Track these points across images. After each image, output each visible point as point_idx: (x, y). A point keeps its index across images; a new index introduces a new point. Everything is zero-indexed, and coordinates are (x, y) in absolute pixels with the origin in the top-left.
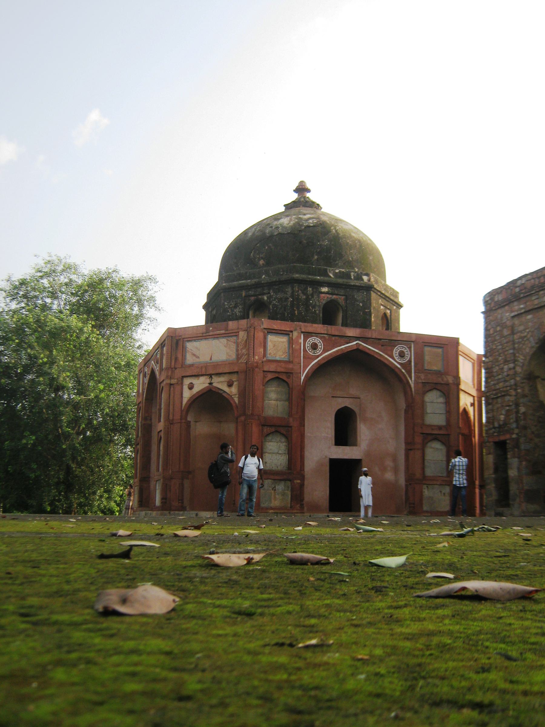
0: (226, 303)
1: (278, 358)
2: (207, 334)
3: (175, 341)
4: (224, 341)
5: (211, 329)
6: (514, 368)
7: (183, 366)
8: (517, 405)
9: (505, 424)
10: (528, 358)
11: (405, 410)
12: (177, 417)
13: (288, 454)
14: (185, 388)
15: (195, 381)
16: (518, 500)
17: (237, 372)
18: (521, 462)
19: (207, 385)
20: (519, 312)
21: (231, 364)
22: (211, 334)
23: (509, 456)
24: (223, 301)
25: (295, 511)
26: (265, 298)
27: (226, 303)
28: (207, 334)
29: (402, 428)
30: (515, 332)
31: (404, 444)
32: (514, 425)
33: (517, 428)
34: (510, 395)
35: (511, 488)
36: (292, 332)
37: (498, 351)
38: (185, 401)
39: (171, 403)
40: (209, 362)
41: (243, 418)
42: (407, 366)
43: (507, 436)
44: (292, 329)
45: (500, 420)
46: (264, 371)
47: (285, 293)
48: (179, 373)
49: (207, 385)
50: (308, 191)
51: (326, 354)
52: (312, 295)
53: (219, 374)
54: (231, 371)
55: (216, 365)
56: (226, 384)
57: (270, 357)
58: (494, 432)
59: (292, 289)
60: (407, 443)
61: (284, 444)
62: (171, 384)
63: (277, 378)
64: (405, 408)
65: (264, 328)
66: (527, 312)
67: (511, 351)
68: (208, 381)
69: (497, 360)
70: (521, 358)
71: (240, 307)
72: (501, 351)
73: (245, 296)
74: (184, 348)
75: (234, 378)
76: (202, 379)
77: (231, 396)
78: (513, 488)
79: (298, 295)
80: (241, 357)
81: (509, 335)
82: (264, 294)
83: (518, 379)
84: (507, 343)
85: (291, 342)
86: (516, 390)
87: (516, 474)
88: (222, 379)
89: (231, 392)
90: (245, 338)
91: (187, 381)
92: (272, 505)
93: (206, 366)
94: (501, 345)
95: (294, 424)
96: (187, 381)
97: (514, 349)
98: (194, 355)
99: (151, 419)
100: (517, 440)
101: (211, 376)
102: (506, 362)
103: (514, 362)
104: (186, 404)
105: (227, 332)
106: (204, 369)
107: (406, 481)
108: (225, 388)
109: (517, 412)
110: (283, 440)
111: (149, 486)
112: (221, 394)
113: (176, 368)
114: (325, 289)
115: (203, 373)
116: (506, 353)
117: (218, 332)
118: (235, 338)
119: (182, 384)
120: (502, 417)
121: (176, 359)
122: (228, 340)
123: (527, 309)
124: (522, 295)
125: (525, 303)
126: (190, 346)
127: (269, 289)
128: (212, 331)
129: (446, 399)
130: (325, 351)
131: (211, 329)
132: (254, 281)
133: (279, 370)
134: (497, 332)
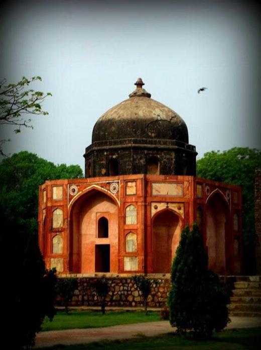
4: (175, 185)
15: (158, 205)
17: (183, 203)
21: (180, 198)
22: (168, 180)
26: (159, 156)
38: (152, 215)
42: (229, 200)
55: (171, 198)
68: (166, 205)
74: (151, 187)
75: (182, 205)
76: (162, 204)
80: (186, 195)
82: (158, 154)
85: (203, 188)
90: (188, 185)
91: (153, 205)
101: (167, 203)
119: (151, 206)
126: (154, 185)
127: (161, 152)
128: (169, 179)
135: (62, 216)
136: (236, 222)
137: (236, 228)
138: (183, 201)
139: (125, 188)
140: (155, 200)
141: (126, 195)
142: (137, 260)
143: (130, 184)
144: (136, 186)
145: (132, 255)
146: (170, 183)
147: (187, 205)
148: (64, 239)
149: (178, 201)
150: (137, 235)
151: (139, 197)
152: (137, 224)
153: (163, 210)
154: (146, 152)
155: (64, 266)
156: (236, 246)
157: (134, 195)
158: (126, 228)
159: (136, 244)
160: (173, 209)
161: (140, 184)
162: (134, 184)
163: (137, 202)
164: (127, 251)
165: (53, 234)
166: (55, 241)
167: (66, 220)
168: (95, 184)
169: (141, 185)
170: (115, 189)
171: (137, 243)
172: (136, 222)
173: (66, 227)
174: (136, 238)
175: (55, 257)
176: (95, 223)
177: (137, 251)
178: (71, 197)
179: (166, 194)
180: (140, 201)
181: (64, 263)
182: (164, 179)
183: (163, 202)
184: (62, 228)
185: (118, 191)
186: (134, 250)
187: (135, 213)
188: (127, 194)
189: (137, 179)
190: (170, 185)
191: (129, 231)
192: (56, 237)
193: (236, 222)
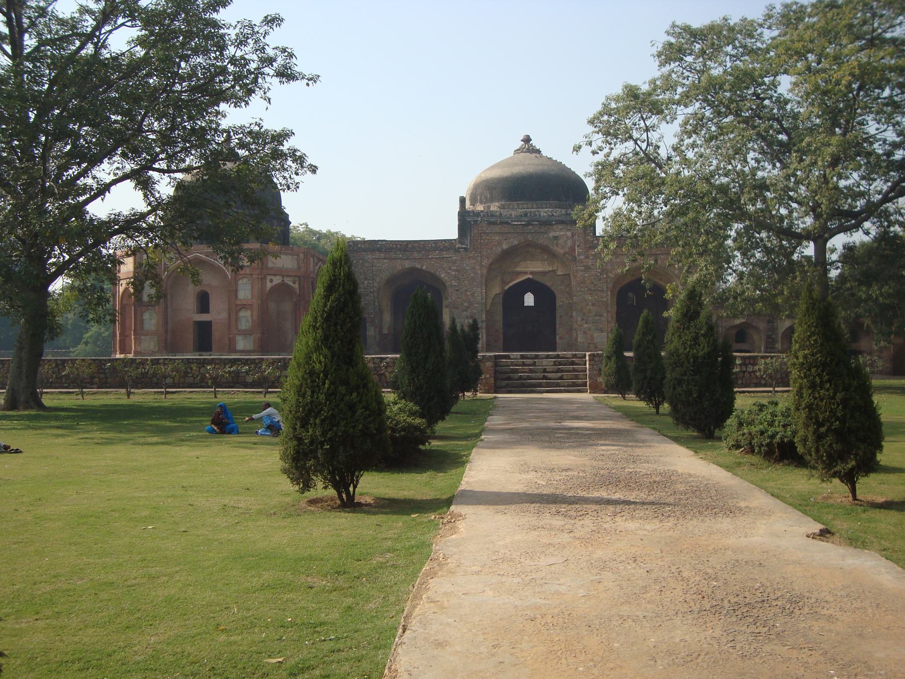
15: (272, 277)
38: (268, 289)
53: (288, 276)
70: (378, 279)
76: (278, 277)
91: (269, 278)
96: (269, 278)
102: (366, 279)
108: (291, 284)
142: (252, 338)
145: (246, 333)
150: (252, 311)
158: (238, 303)
172: (250, 297)
187: (249, 287)
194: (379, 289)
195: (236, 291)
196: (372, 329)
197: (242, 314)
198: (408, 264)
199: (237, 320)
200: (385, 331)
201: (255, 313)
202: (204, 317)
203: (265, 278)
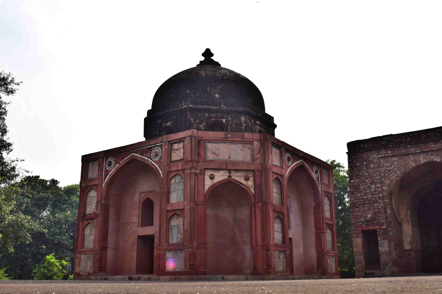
0: (192, 119)
1: (276, 164)
2: (226, 139)
3: (197, 141)
4: (241, 146)
5: (229, 136)
6: (381, 187)
7: (205, 161)
8: (385, 209)
9: (373, 219)
10: (394, 182)
11: (315, 208)
12: (201, 199)
13: (283, 232)
14: (207, 178)
15: (216, 174)
16: (389, 265)
17: (253, 171)
18: (389, 243)
19: (227, 177)
20: (386, 155)
21: (248, 163)
23: (379, 239)
24: (189, 117)
25: (288, 274)
26: (224, 121)
27: (192, 119)
28: (226, 139)
29: (312, 219)
30: (381, 166)
31: (314, 230)
32: (384, 221)
33: (386, 222)
34: (379, 203)
35: (381, 258)
36: (281, 147)
37: (365, 176)
39: (196, 188)
40: (228, 160)
41: (260, 205)
42: (318, 178)
43: (377, 227)
44: (282, 146)
45: (367, 217)
46: (273, 172)
47: (240, 120)
48: (202, 165)
49: (227, 177)
50: (212, 55)
51: (293, 165)
52: (254, 125)
53: (237, 170)
54: (249, 169)
55: (235, 163)
56: (243, 178)
57: (274, 163)
58: (362, 224)
59: (246, 118)
60: (315, 228)
61: (280, 225)
62: (195, 174)
63: (277, 179)
64: (314, 206)
65: (272, 142)
66: (393, 156)
67: (379, 177)
68: (228, 174)
69: (364, 182)
71: (204, 124)
72: (367, 176)
73: (208, 117)
74: (205, 147)
76: (222, 173)
77: (248, 187)
78: (383, 258)
79: (248, 123)
80: (256, 160)
81: (376, 167)
82: (224, 118)
83: (385, 194)
84: (374, 172)
86: (383, 200)
87: (387, 249)
88: (239, 174)
89: (248, 185)
90: (259, 146)
91: (208, 173)
92: (279, 270)
93: (226, 163)
94: (367, 173)
95: (285, 212)
97: (381, 176)
98: (215, 153)
99: (109, 200)
100: (387, 229)
101: (230, 171)
102: (372, 183)
103: (381, 184)
104: (208, 190)
105: (243, 140)
106: (224, 165)
107: (317, 253)
109: (386, 213)
110: (280, 222)
111: (107, 254)
112: (239, 185)
113: (198, 162)
114: (258, 123)
115: (224, 168)
116: (373, 178)
117: (236, 139)
118: (249, 145)
119: (204, 175)
120: (369, 216)
121: (199, 154)
122: (244, 146)
123: (395, 154)
124: (390, 146)
125: (393, 151)
127: (228, 115)
129: (330, 202)
130: (292, 164)
131: (229, 136)
132: (216, 108)
133: (279, 172)
134: (363, 165)
135: (96, 198)
136: (327, 207)
137: (327, 214)
138: (252, 168)
139: (170, 151)
140: (210, 167)
141: (171, 161)
142: (182, 255)
143: (176, 146)
144: (183, 148)
145: (176, 248)
146: (233, 142)
147: (258, 174)
148: (96, 229)
149: (245, 168)
150: (184, 218)
151: (187, 162)
152: (184, 201)
153: (222, 180)
154: (207, 115)
155: (94, 263)
156: (328, 236)
157: (181, 160)
158: (169, 208)
159: (182, 232)
160: (238, 179)
161: (188, 144)
162: (181, 145)
163: (184, 170)
164: (170, 243)
165: (86, 223)
166: (87, 231)
167: (100, 203)
168: (134, 152)
169: (189, 145)
170: (156, 155)
171: (184, 230)
172: (182, 200)
173: (100, 212)
174: (182, 223)
175: (84, 253)
176: (138, 205)
177: (184, 242)
178: (107, 172)
179: (226, 158)
180: (188, 167)
181: (94, 260)
182: (224, 136)
183: (222, 170)
184: (94, 213)
185: (161, 158)
186: (179, 241)
187: (181, 186)
188: (173, 160)
189: (185, 138)
190: (233, 146)
191: (173, 213)
192: (88, 226)
193: (327, 207)
194: (391, 194)
195: (168, 193)
196: (386, 243)
197: (175, 222)
198: (423, 159)
199: (168, 229)
200: (407, 247)
201: (187, 219)
202: (148, 231)
203: (203, 173)
